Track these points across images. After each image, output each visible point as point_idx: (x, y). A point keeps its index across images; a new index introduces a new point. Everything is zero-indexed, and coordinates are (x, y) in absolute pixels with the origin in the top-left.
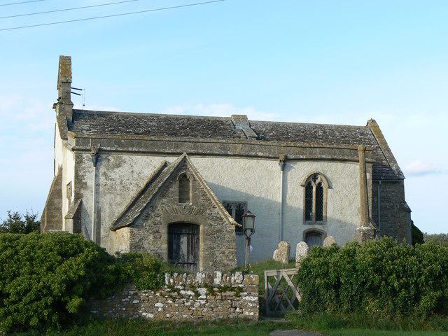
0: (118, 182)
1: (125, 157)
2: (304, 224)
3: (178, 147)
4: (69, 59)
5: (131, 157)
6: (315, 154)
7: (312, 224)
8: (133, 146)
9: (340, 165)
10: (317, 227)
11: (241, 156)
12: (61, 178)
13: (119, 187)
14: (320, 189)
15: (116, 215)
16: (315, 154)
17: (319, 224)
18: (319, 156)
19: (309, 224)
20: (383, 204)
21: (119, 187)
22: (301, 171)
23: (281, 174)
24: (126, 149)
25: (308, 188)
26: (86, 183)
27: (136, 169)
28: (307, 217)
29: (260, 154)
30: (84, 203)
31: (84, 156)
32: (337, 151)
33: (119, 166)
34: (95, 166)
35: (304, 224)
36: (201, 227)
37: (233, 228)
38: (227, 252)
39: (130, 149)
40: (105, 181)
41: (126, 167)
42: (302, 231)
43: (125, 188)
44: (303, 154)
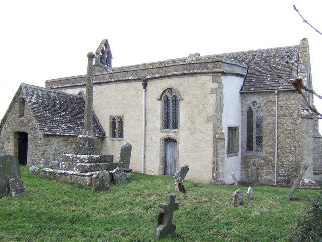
2: (161, 132)
4: (107, 41)
6: (169, 72)
7: (168, 132)
9: (191, 79)
10: (171, 134)
11: (119, 81)
14: (176, 102)
16: (169, 72)
17: (173, 132)
18: (172, 73)
19: (166, 131)
20: (281, 112)
22: (157, 88)
23: (144, 92)
25: (166, 102)
28: (166, 125)
29: (130, 78)
32: (188, 67)
35: (161, 132)
36: (29, 135)
37: (42, 136)
38: (39, 153)
42: (160, 138)
44: (159, 73)
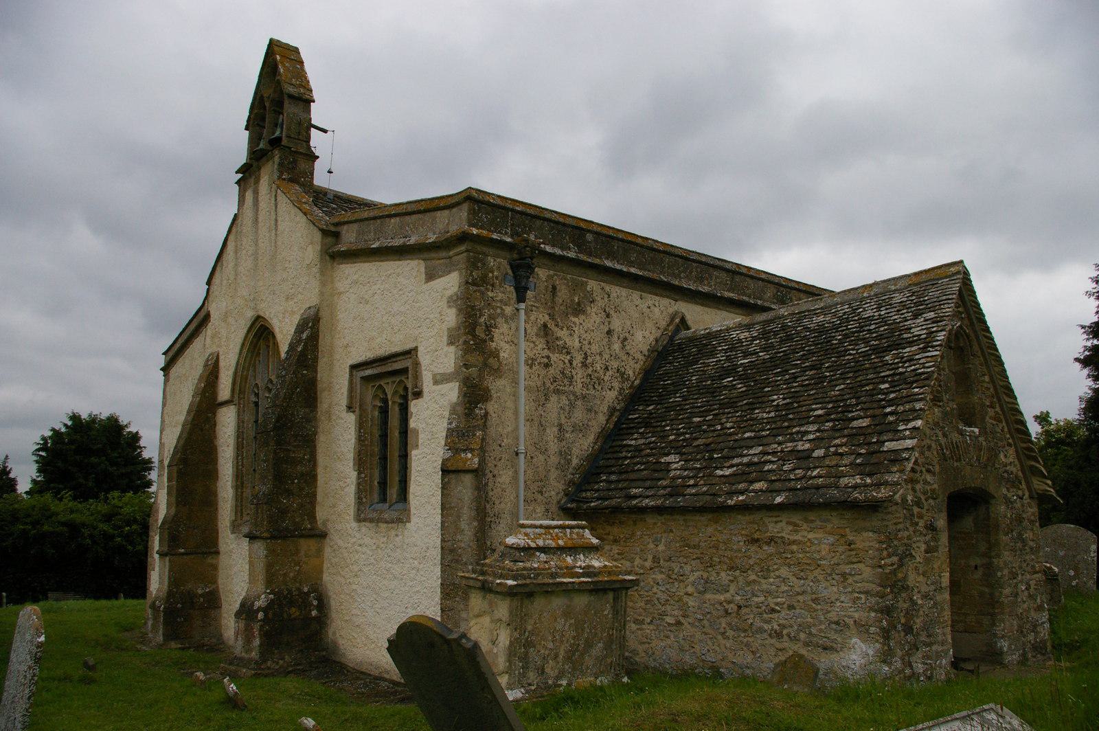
0: (579, 358)
1: (593, 285)
3: (700, 280)
5: (607, 288)
8: (612, 255)
12: (316, 347)
13: (579, 375)
15: (575, 461)
21: (579, 375)
24: (597, 261)
26: (495, 354)
27: (616, 324)
30: (493, 419)
31: (491, 262)
33: (578, 310)
34: (521, 298)
39: (608, 263)
40: (546, 352)
41: (594, 317)
43: (594, 381)
